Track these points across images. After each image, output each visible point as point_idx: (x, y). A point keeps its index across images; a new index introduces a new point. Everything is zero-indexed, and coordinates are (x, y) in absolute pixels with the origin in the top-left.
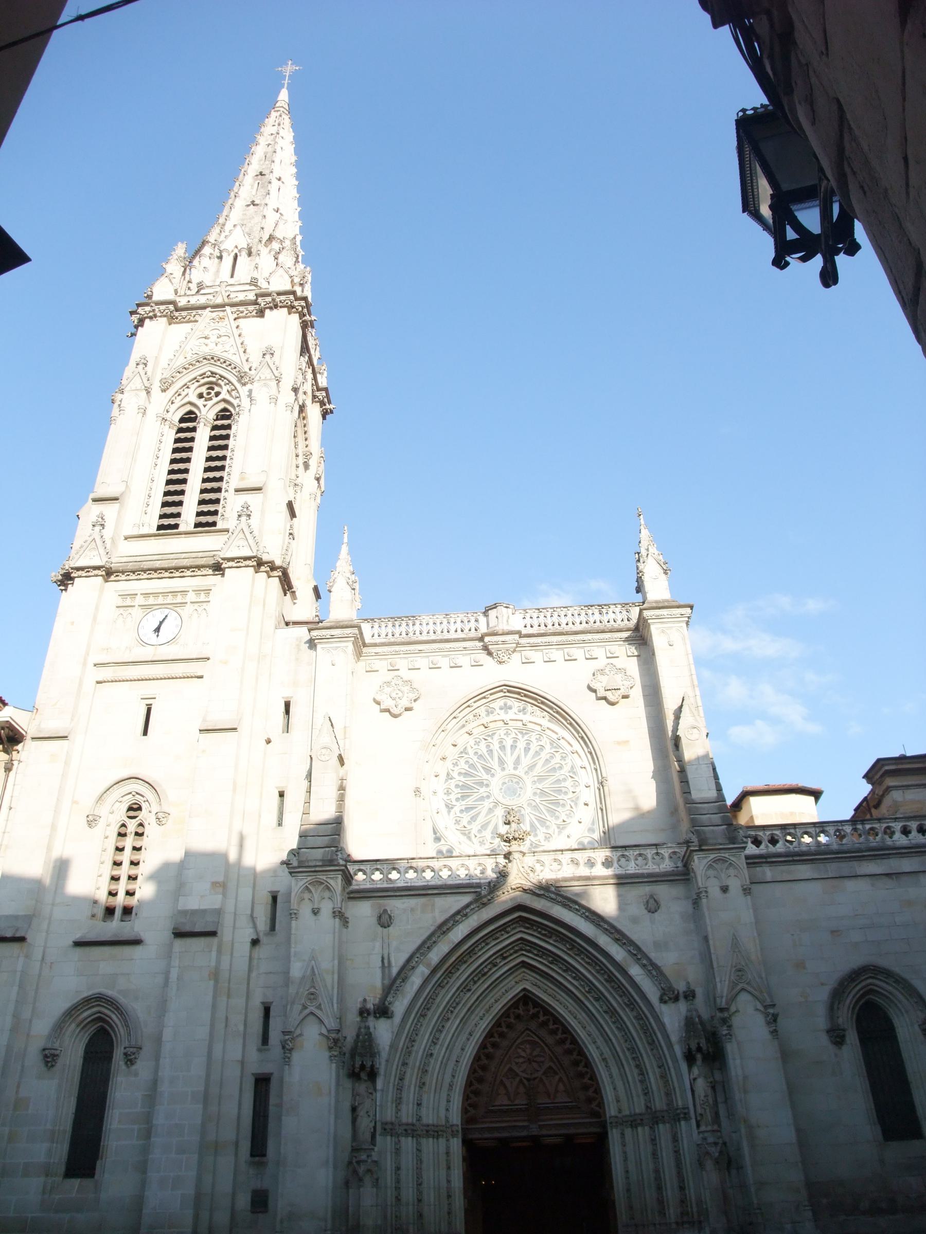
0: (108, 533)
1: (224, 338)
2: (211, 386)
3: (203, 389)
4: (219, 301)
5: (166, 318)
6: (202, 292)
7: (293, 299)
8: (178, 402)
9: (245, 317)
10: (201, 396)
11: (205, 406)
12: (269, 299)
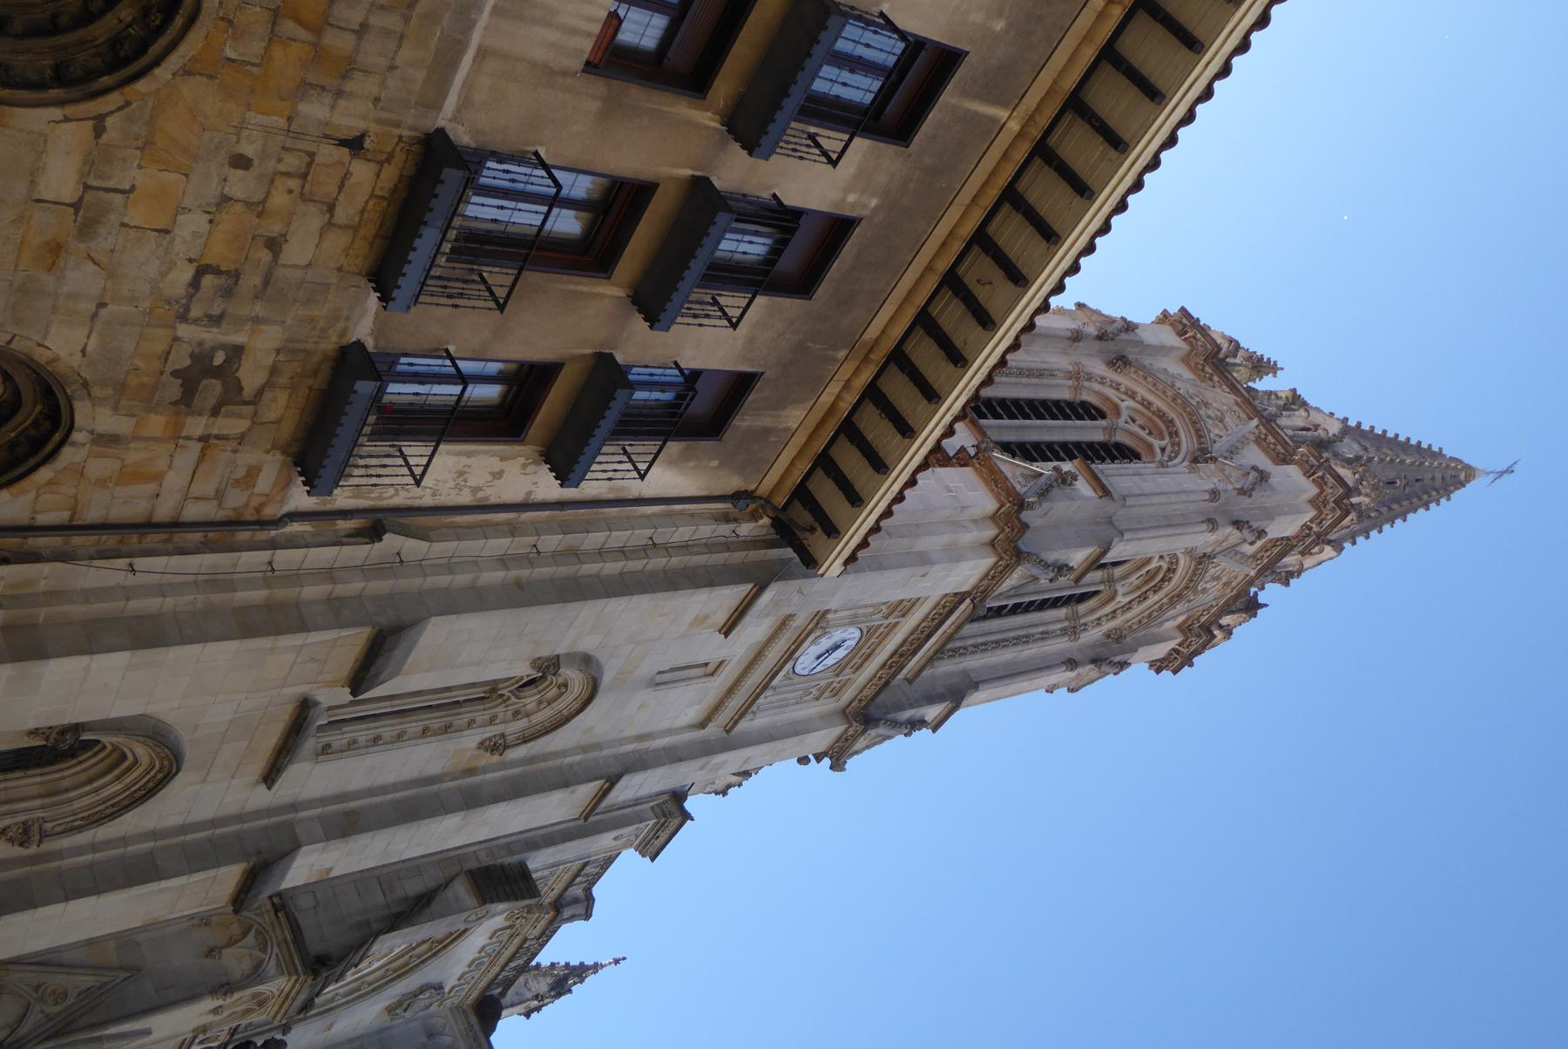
5: (1189, 348)
8: (1111, 393)
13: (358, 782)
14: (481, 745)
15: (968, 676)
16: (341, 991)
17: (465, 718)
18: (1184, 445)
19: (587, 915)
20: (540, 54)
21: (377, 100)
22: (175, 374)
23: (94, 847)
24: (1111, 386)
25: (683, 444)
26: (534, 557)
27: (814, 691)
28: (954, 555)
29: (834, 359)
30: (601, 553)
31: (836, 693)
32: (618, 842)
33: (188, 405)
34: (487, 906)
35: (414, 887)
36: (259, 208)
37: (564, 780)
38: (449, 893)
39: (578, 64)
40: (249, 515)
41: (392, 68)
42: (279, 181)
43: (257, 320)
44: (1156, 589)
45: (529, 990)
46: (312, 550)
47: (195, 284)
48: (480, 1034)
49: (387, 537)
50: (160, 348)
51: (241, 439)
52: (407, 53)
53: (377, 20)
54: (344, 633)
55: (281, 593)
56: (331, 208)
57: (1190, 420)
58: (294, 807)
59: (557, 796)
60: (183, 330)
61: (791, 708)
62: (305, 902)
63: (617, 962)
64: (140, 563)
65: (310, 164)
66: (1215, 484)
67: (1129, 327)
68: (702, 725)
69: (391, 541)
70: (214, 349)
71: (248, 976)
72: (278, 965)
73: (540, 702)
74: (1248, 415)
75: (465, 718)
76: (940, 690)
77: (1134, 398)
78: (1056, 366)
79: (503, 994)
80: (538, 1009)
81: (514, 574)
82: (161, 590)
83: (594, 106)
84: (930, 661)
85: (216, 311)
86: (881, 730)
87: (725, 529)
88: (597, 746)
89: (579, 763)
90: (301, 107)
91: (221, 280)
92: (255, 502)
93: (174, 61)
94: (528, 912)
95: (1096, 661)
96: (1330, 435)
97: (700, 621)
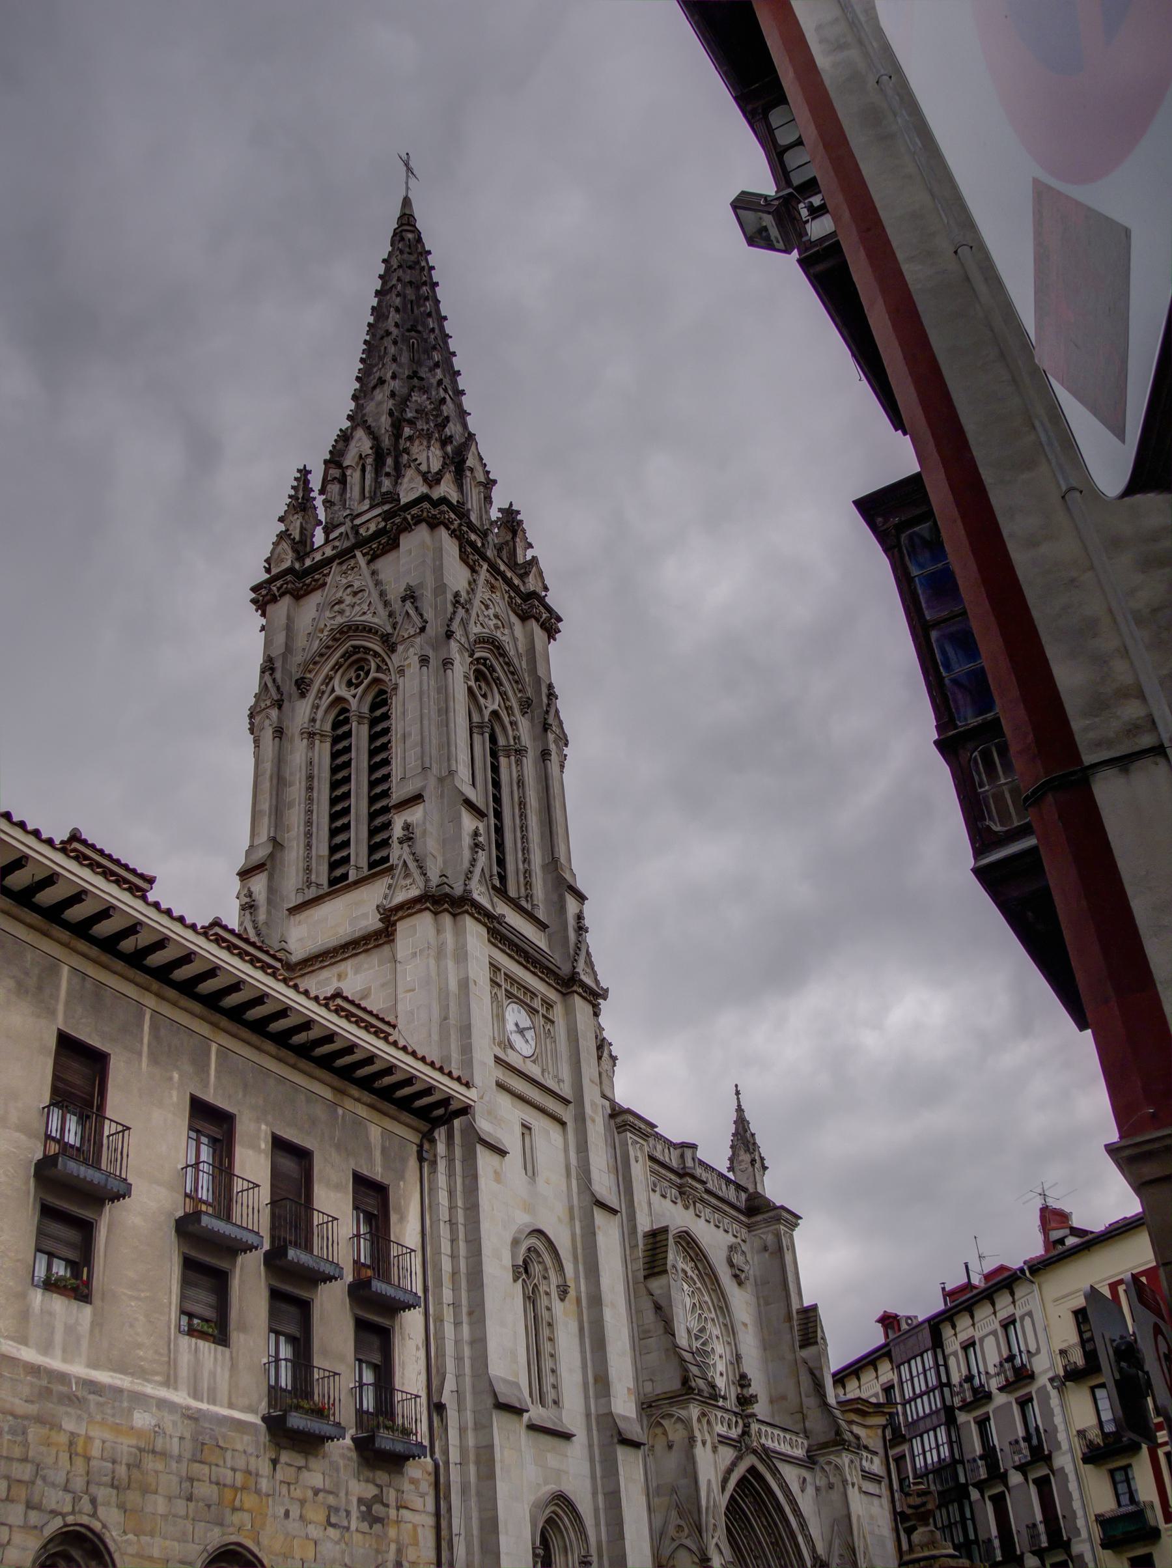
0: (262, 916)
2: (361, 667)
3: (352, 674)
4: (347, 544)
7: (428, 506)
8: (326, 702)
10: (350, 684)
11: (354, 696)
12: (398, 520)
13: (577, 1377)
14: (562, 1300)
15: (547, 864)
17: (545, 1314)
19: (693, 1147)
21: (257, 1457)
22: (371, 1528)
23: (597, 1525)
24: (321, 698)
25: (392, 1212)
26: (456, 1305)
27: (548, 1027)
28: (461, 956)
29: (344, 1116)
30: (454, 1257)
31: (549, 1005)
32: (640, 1159)
33: (383, 1519)
34: (669, 1267)
35: (650, 1316)
36: (303, 1502)
37: (590, 1234)
38: (657, 1292)
40: (432, 1479)
41: (245, 1452)
42: (292, 1496)
43: (347, 1494)
44: (492, 669)
45: (747, 1169)
46: (450, 1442)
47: (333, 1526)
48: (771, 1214)
49: (443, 1401)
50: (360, 1536)
51: (398, 1491)
52: (239, 1447)
53: (229, 1464)
54: (495, 1424)
55: (472, 1457)
56: (299, 1468)
57: (355, 631)
58: (588, 1415)
59: (601, 1239)
60: (353, 1527)
62: (648, 1387)
63: (738, 1093)
64: (455, 1530)
65: (284, 1482)
66: (415, 654)
67: (269, 667)
68: (563, 1124)
69: (447, 1398)
70: (360, 1512)
71: (686, 1426)
72: (683, 1408)
73: (540, 1262)
76: (555, 897)
77: (331, 679)
78: (304, 758)
79: (745, 1190)
80: (762, 1159)
81: (465, 1318)
82: (468, 1519)
83: (242, 1337)
84: (530, 916)
85: (345, 1514)
86: (581, 966)
87: (442, 1165)
88: (571, 1209)
89: (581, 1221)
90: (264, 1490)
91: (332, 1514)
92: (426, 1476)
93: (255, 1550)
94: (684, 1194)
95: (546, 727)
96: (370, 452)
97: (498, 1176)
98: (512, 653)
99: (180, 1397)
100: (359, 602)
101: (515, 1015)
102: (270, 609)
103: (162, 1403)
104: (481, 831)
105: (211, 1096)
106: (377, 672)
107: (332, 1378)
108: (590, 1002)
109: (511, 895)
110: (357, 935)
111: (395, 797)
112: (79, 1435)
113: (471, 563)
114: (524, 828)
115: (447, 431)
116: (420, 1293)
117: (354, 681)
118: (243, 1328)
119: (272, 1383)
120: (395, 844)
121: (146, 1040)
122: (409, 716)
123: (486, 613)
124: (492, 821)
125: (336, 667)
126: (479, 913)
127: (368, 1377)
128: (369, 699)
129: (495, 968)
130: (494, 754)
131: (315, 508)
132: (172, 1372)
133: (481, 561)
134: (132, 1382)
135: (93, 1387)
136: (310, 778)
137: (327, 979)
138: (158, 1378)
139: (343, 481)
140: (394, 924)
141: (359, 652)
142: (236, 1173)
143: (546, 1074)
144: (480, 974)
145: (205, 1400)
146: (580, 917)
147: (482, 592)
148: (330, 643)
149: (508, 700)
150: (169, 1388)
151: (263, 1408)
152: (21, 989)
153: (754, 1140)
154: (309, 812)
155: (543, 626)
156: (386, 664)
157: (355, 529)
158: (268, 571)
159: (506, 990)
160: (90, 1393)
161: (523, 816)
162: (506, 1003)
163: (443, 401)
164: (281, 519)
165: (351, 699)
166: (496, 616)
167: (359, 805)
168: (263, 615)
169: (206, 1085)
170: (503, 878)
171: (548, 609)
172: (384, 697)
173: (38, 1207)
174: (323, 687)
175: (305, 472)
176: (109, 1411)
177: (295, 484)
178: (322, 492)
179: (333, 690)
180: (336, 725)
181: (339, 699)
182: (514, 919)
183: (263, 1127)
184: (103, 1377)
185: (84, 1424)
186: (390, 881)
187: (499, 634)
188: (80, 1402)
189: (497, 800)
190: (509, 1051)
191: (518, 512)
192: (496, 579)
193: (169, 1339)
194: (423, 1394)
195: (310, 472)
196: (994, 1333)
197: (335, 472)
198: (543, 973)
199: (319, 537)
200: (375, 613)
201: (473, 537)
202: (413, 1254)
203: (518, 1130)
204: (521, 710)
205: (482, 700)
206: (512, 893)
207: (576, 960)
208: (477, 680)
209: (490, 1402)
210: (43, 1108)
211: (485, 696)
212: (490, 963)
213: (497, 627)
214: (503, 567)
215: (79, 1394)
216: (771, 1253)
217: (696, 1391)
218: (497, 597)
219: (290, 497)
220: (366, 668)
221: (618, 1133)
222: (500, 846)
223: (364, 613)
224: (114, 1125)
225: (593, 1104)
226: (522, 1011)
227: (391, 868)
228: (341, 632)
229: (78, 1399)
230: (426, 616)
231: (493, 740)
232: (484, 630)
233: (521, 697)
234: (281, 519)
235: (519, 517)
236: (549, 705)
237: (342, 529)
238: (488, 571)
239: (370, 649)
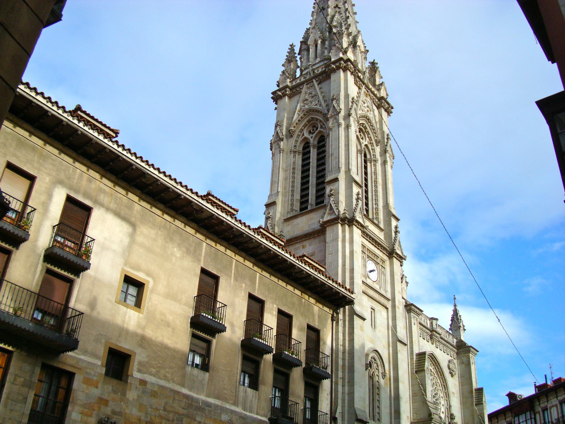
1: (315, 97)
3: (311, 128)
6: (304, 73)
8: (300, 139)
9: (322, 82)
10: (310, 132)
16: (444, 390)
18: (321, 119)
19: (437, 319)
20: (257, 401)
26: (343, 378)
29: (305, 302)
30: (344, 359)
31: (383, 262)
32: (416, 324)
34: (425, 368)
39: (257, 392)
44: (366, 128)
49: (336, 416)
59: (399, 356)
61: (386, 279)
68: (387, 308)
69: (338, 415)
73: (375, 363)
74: (311, 82)
75: (377, 396)
80: (464, 326)
81: (346, 384)
83: (263, 387)
84: (377, 226)
86: (396, 247)
87: (341, 323)
98: (374, 122)
99: (239, 409)
100: (314, 100)
101: (371, 265)
102: (279, 102)
103: (232, 412)
104: (360, 193)
105: (256, 294)
106: (321, 128)
107: (295, 405)
108: (399, 261)
109: (370, 218)
110: (311, 231)
111: (328, 179)
112: (201, 422)
113: (359, 85)
114: (376, 191)
115: (350, 31)
116: (330, 373)
117: (312, 131)
118: (264, 384)
119: (273, 405)
120: (327, 197)
121: (233, 272)
122: (333, 147)
123: (364, 105)
124: (364, 188)
125: (305, 126)
126: (358, 225)
127: (308, 405)
128: (317, 138)
129: (363, 246)
130: (365, 162)
131: (297, 61)
132: (237, 400)
133: (362, 84)
134: (222, 403)
135: (209, 405)
136: (294, 169)
137: (298, 247)
138: (231, 402)
139: (308, 50)
140: (325, 228)
141: (314, 120)
142: (264, 323)
143: (381, 289)
144: (358, 249)
145: (248, 411)
146: (396, 227)
147: (363, 97)
148: (303, 116)
149: (371, 140)
150: (235, 406)
151: (269, 415)
152: (188, 252)
153: (461, 318)
154: (293, 182)
155: (386, 110)
156: (325, 125)
157: (313, 71)
158: (278, 86)
159: (367, 255)
160: (206, 406)
161: (376, 186)
162: (367, 259)
163: (348, 17)
164: (283, 65)
165: (310, 138)
166: (368, 107)
167: (313, 180)
168: (276, 103)
169: (255, 289)
170: (367, 211)
171: (388, 104)
172: (323, 138)
173: (191, 335)
174: (300, 133)
175: (292, 46)
176: (213, 414)
177: (289, 51)
178: (299, 54)
179: (303, 135)
180: (304, 149)
181: (306, 138)
182: (372, 227)
183: (275, 306)
184: (211, 400)
185: (204, 419)
186: (324, 211)
187: (369, 114)
188: (202, 410)
189: (366, 180)
190: (368, 279)
191: (377, 64)
192: (368, 92)
193: (236, 386)
194: (329, 413)
195: (295, 46)
196: (556, 406)
197: (304, 47)
198: (381, 249)
199: (298, 74)
200: (320, 105)
201: (360, 74)
202: (328, 357)
203: (370, 310)
204: (376, 144)
205: (361, 140)
206: (371, 216)
207: (394, 244)
208: (360, 132)
209: (354, 418)
210: (195, 297)
211: (362, 138)
212: (362, 245)
213: (368, 111)
214: (371, 87)
215: (202, 407)
216: (465, 365)
217: (434, 420)
218: (368, 99)
219: (287, 56)
220: (316, 126)
221: (408, 313)
222: (367, 198)
223: (316, 105)
224: (221, 304)
225: (399, 301)
226: (373, 263)
227: (325, 206)
228: (307, 112)
229: (202, 408)
230: (341, 107)
231: (365, 156)
232: (363, 113)
233: (377, 139)
234: (283, 65)
235: (377, 66)
236: (387, 143)
237: (307, 70)
238: (365, 88)
239: (318, 119)
